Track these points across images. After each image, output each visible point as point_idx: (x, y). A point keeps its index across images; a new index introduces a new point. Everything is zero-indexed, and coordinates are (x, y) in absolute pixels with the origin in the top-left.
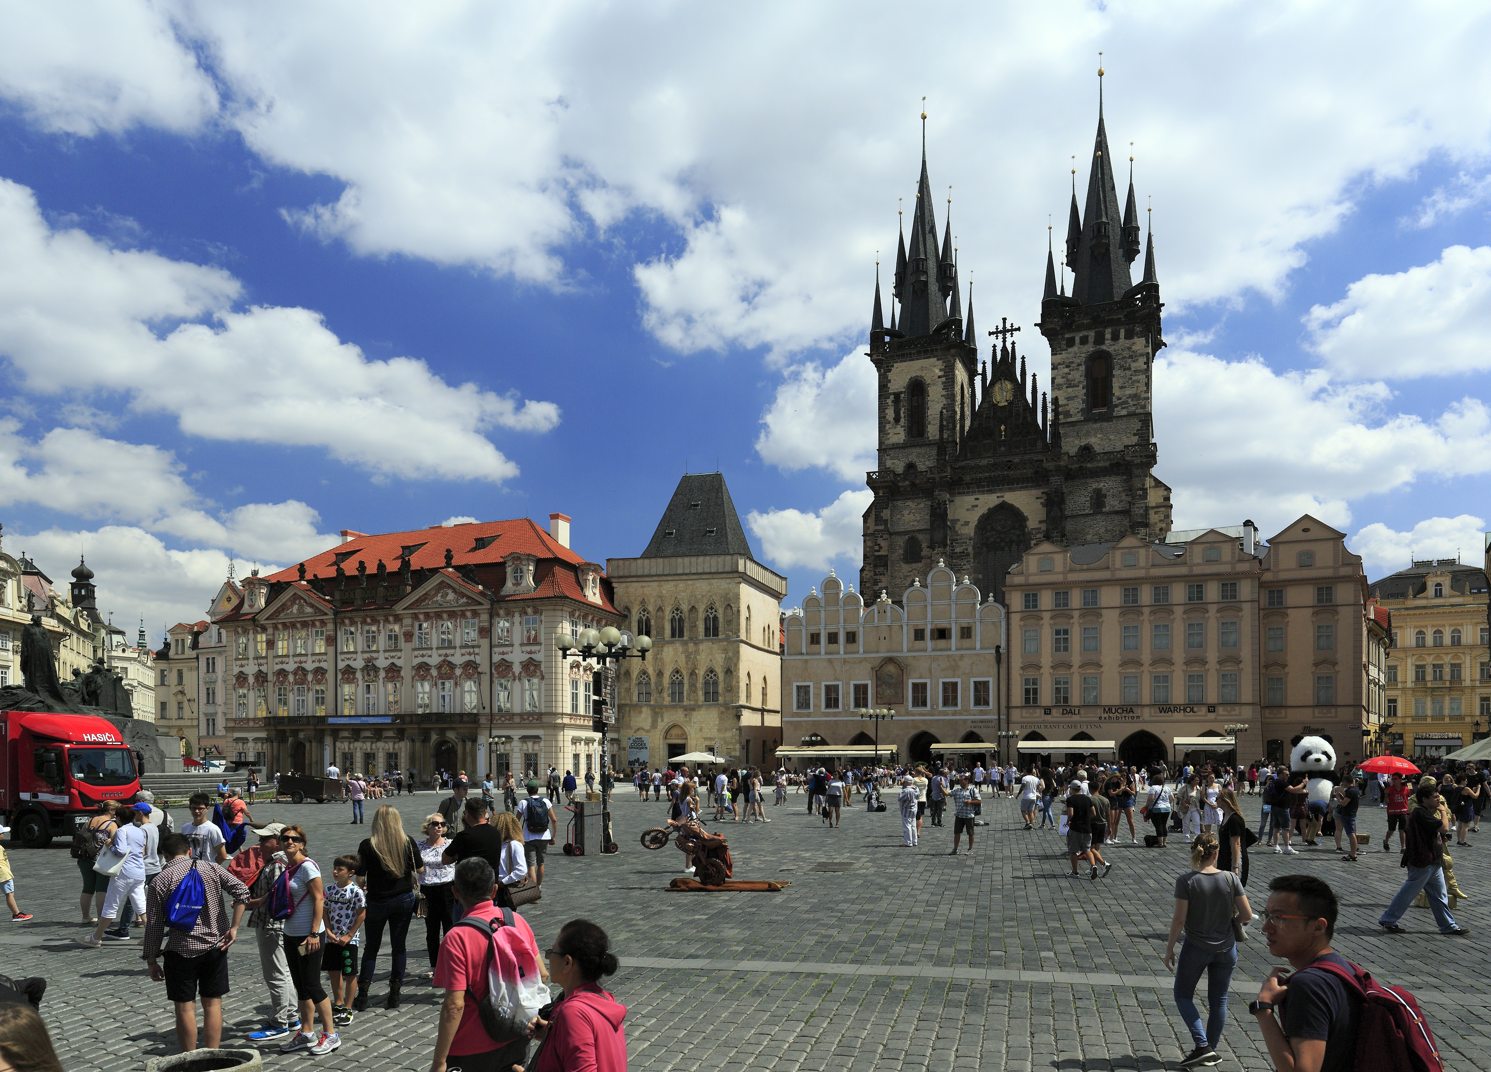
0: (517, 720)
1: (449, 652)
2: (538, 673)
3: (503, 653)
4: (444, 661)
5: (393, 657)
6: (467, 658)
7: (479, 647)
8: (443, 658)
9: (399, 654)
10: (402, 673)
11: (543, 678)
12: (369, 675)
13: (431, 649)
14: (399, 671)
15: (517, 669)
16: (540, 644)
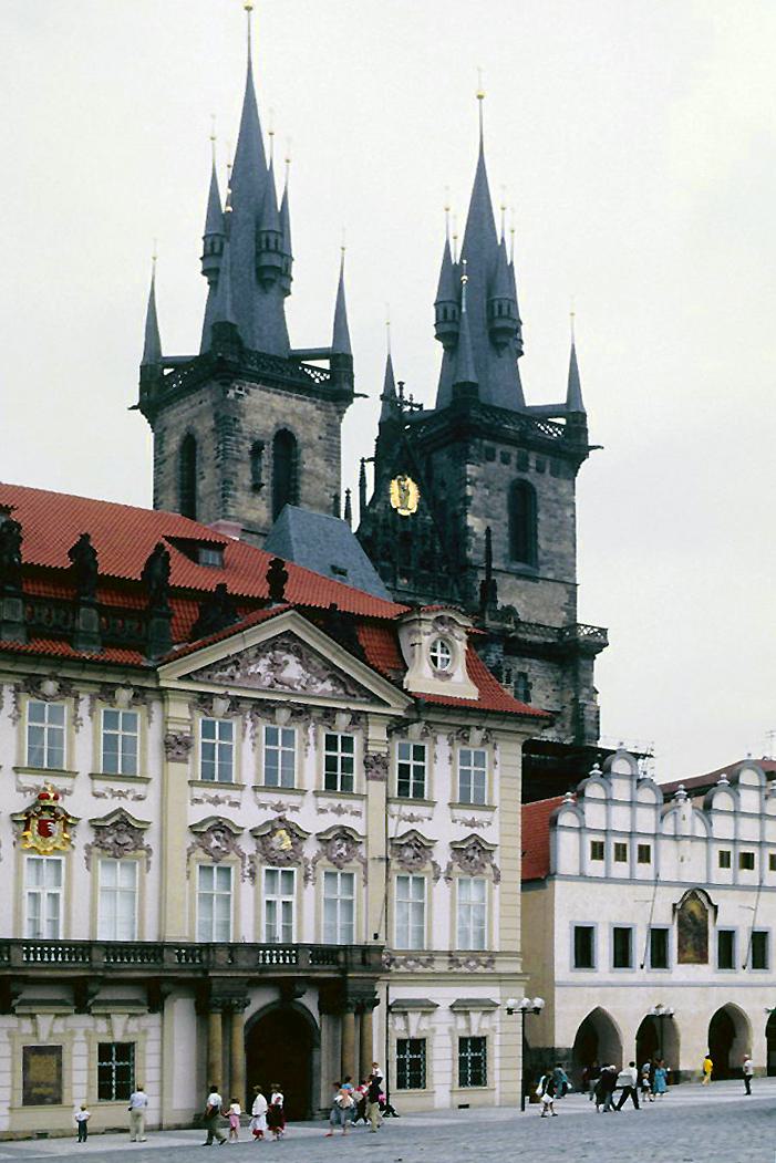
0: (441, 966)
1: (286, 799)
2: (489, 870)
3: (411, 819)
4: (281, 820)
5: (121, 794)
6: (332, 820)
7: (363, 797)
8: (272, 815)
9: (139, 789)
10: (150, 839)
11: (497, 879)
12: (45, 832)
13: (241, 787)
14: (141, 830)
15: (442, 856)
16: (492, 808)
